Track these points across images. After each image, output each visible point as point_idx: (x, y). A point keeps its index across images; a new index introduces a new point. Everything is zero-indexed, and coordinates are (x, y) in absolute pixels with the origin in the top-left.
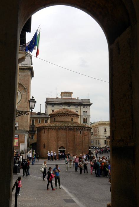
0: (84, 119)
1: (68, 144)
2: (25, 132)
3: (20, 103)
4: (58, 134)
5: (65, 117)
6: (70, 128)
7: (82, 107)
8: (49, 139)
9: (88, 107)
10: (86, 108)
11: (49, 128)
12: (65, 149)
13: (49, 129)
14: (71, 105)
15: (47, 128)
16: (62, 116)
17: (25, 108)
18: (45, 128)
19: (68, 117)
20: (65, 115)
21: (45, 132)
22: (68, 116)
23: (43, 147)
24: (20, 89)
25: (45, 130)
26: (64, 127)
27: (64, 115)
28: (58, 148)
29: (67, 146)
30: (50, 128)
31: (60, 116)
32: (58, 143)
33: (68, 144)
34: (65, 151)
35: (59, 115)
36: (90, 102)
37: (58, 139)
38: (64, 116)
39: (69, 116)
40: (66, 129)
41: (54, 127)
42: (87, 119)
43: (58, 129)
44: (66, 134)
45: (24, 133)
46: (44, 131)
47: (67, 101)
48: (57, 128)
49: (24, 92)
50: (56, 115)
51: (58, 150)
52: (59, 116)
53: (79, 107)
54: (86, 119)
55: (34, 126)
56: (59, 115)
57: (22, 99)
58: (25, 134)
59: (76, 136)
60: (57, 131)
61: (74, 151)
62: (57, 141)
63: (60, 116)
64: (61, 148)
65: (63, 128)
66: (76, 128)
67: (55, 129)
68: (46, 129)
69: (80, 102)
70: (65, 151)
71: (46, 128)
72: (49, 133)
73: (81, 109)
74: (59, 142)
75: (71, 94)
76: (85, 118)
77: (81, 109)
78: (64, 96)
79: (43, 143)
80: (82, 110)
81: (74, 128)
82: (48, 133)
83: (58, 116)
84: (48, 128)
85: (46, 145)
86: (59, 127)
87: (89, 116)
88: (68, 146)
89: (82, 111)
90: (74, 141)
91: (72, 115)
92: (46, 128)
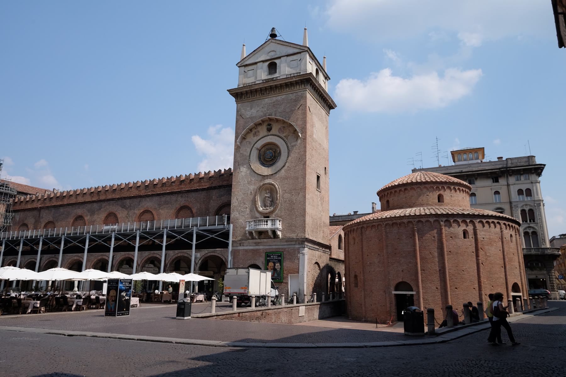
0: (523, 211)
2: (299, 244)
3: (286, 167)
7: (512, 180)
9: (533, 177)
10: (528, 181)
12: (412, 291)
14: (476, 179)
17: (297, 178)
18: (354, 229)
24: (285, 135)
34: (412, 295)
36: (537, 163)
39: (428, 189)
42: (535, 211)
45: (297, 246)
47: (464, 170)
49: (295, 139)
51: (390, 293)
53: (502, 181)
54: (531, 211)
57: (290, 158)
58: (298, 249)
69: (505, 166)
70: (415, 298)
73: (508, 185)
75: (480, 151)
76: (527, 209)
77: (508, 185)
78: (459, 161)
80: (512, 187)
82: (362, 241)
87: (539, 203)
89: (514, 190)
92: (355, 228)
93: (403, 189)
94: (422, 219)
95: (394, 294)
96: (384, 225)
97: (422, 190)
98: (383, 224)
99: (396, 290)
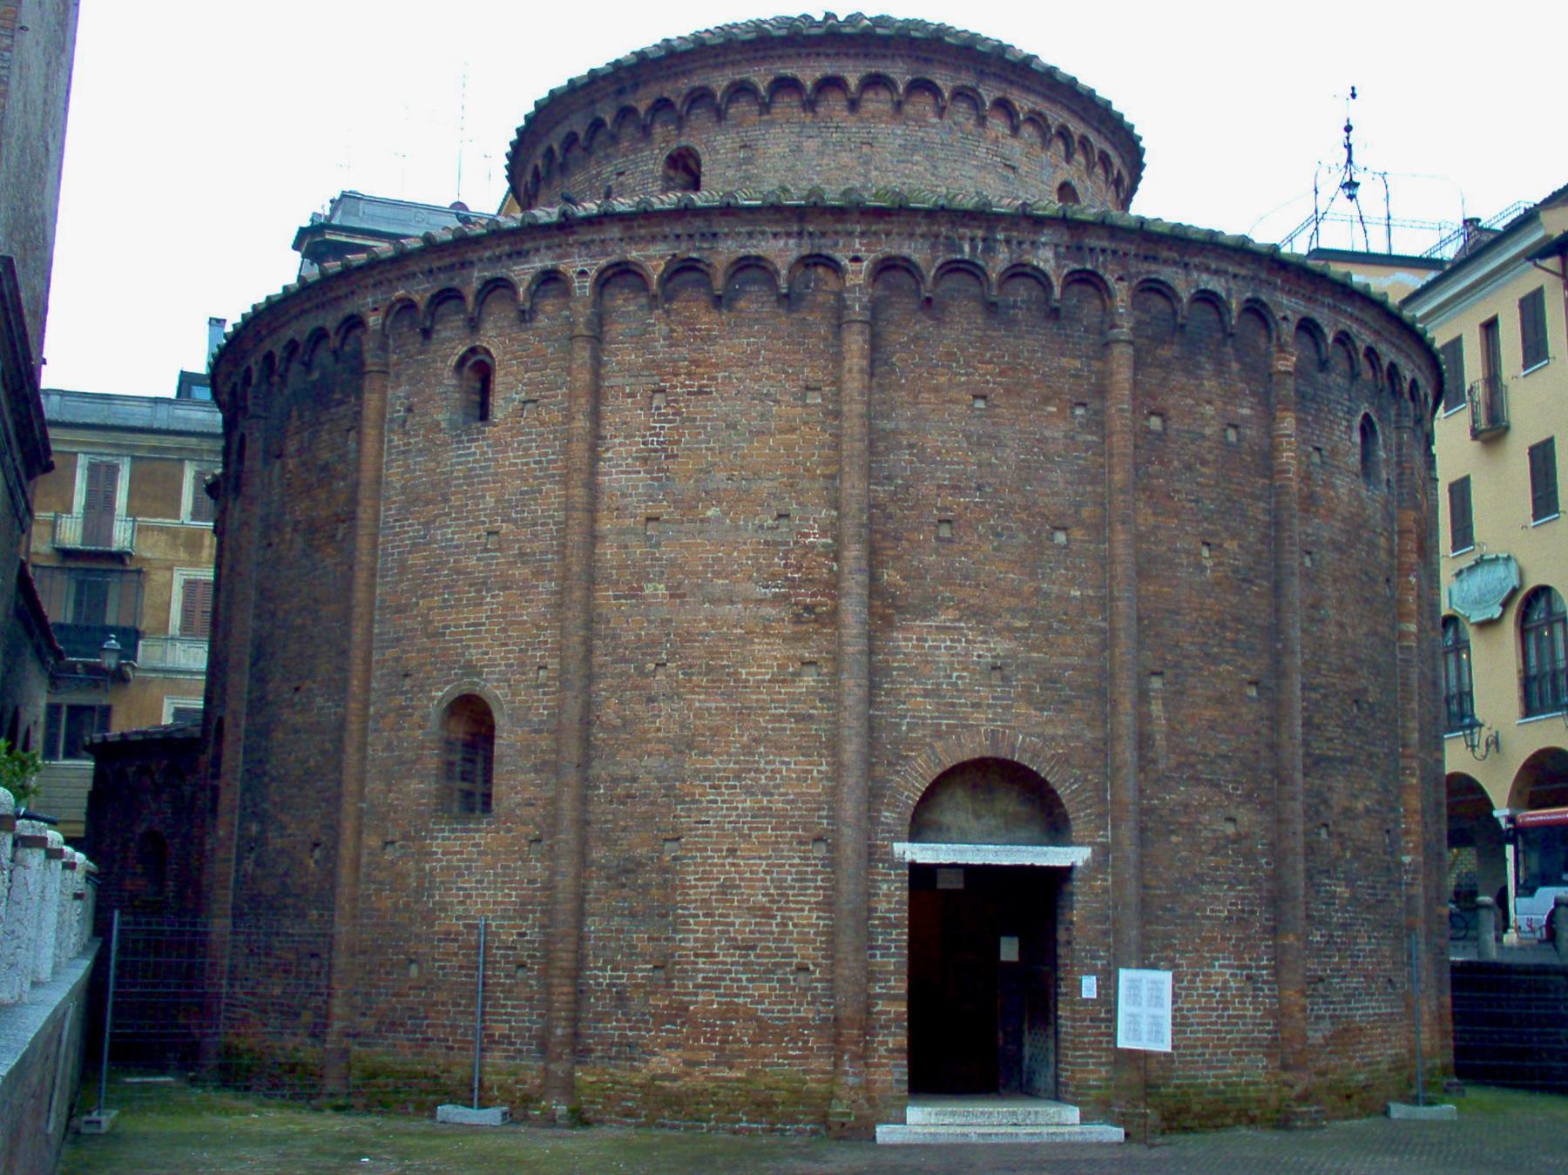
1: (1143, 696)
4: (876, 442)
5: (935, 130)
6: (1183, 284)
8: (608, 552)
11: (621, 274)
13: (624, 303)
15: (550, 279)
16: (877, 102)
18: (498, 286)
19: (998, 125)
20: (945, 81)
21: (499, 379)
22: (1003, 105)
23: (420, 788)
25: (495, 339)
26: (1044, 259)
27: (921, 86)
28: (874, 794)
29: (1126, 753)
30: (653, 257)
31: (835, 105)
32: (875, 676)
33: (1143, 696)
35: (809, 73)
37: (874, 561)
38: (923, 105)
40: (1090, 309)
41: (781, 251)
43: (875, 309)
44: (1098, 423)
46: (480, 371)
48: (857, 275)
50: (720, 82)
51: (873, 855)
52: (786, 105)
55: (120, 557)
56: (809, 73)
59: (1309, 501)
60: (855, 343)
61: (1276, 900)
62: (853, 611)
63: (832, 83)
64: (956, 809)
65: (1018, 272)
66: (1308, 327)
67: (788, 301)
68: (525, 317)
71: (523, 273)
72: (623, 410)
74: (905, 642)
79: (441, 694)
81: (1257, 311)
82: (597, 395)
83: (786, 85)
84: (581, 266)
85: (506, 738)
86: (916, 251)
88: (1143, 741)
90: (1275, 631)
91: (1077, 128)
92: (523, 273)
93: (853, 81)
94: (1167, 274)
95: (914, 867)
96: (865, 264)
97: (982, 121)
98: (856, 259)
99: (915, 836)
